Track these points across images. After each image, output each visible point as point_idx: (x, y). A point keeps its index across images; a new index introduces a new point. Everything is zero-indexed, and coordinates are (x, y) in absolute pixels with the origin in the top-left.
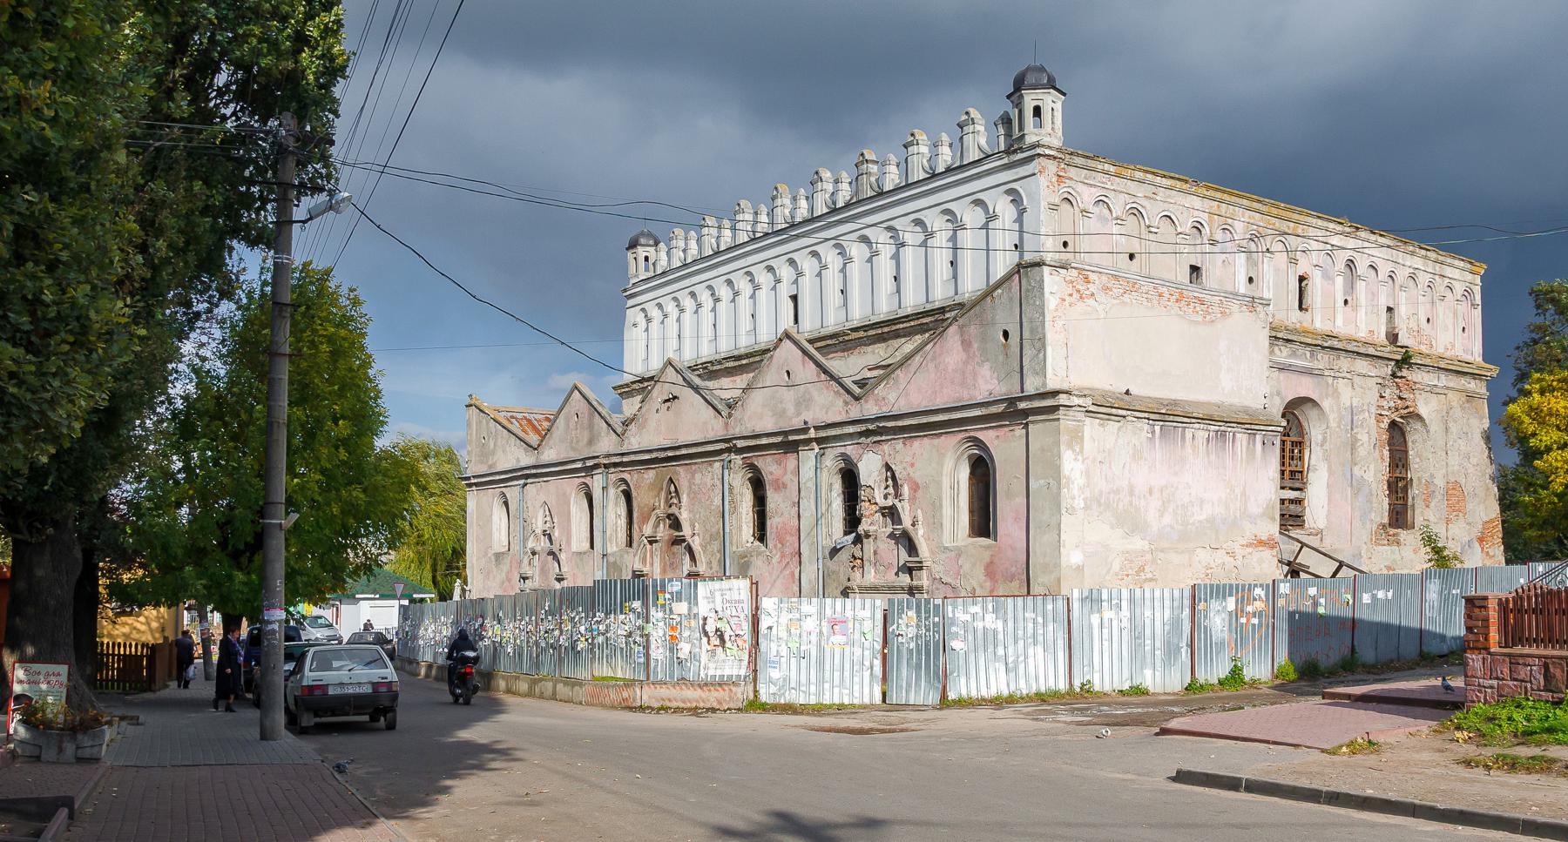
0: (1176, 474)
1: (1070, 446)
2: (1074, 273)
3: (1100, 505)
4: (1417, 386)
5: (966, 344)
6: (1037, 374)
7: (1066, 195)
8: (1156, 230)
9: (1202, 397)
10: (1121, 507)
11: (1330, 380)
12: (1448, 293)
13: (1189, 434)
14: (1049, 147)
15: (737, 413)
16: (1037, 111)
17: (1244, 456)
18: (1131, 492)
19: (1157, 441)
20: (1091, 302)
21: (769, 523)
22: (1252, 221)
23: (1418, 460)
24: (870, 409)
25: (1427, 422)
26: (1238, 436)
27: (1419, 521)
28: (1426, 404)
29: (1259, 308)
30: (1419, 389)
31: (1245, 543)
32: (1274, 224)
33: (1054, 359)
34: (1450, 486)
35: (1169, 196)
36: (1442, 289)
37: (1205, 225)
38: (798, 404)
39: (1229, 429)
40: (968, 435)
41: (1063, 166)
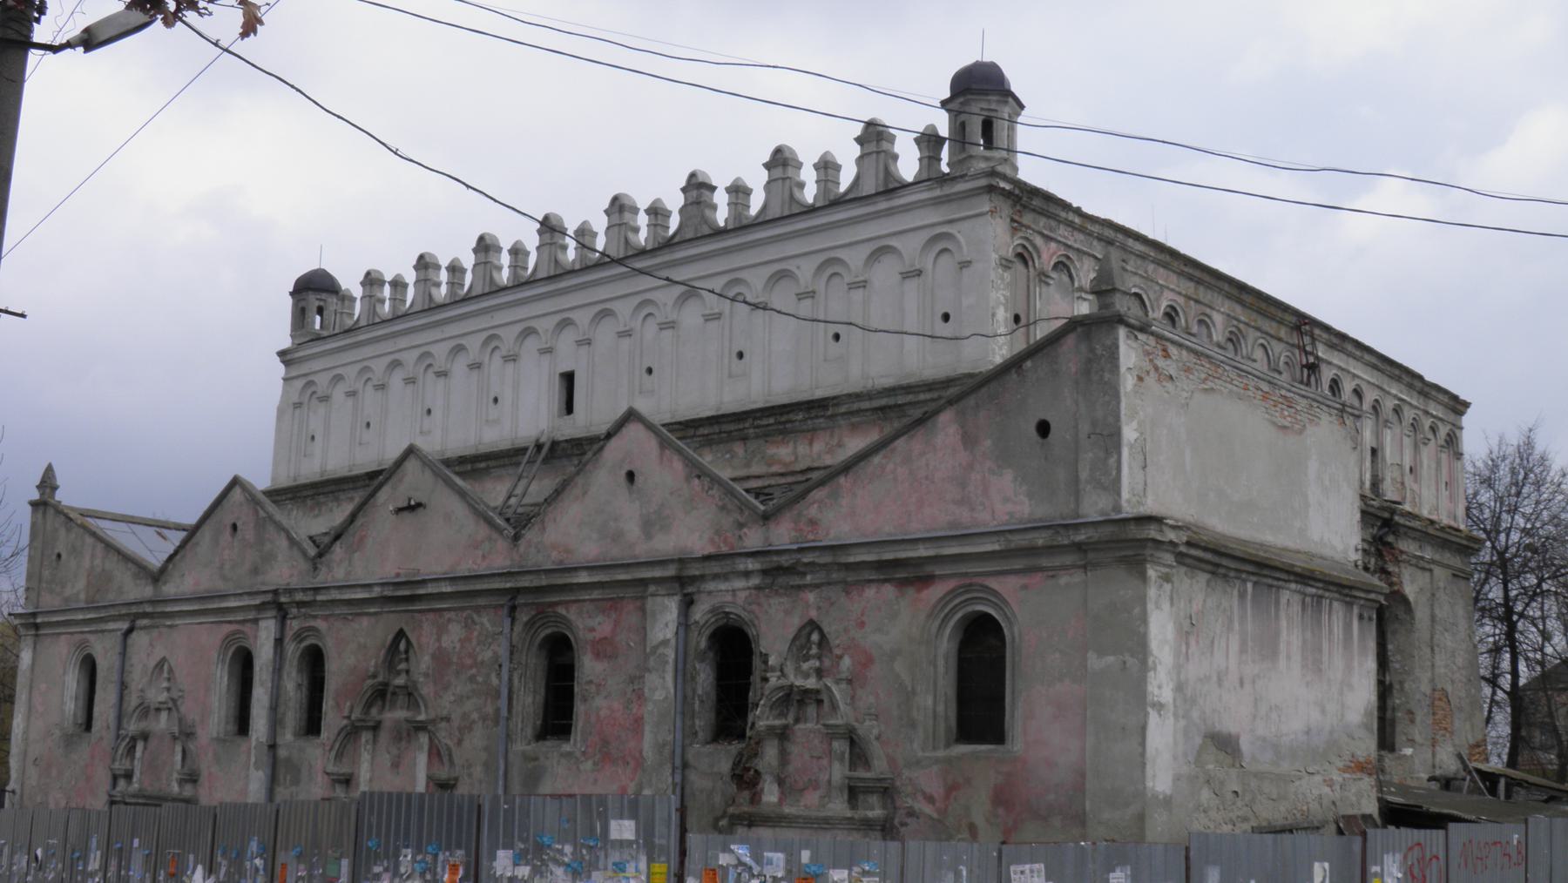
1: (1158, 607)
2: (1152, 341)
5: (969, 440)
6: (1105, 489)
7: (1020, 250)
12: (1430, 436)
13: (1283, 600)
14: (1004, 177)
15: (530, 535)
16: (988, 127)
17: (1341, 636)
20: (1169, 385)
21: (579, 708)
22: (1232, 314)
23: (1398, 657)
24: (782, 534)
25: (1413, 605)
28: (1412, 582)
29: (1349, 421)
30: (1404, 561)
32: (1255, 321)
33: (1130, 468)
34: (1437, 695)
36: (1427, 427)
38: (649, 526)
39: (1327, 594)
40: (968, 581)
41: (1018, 207)
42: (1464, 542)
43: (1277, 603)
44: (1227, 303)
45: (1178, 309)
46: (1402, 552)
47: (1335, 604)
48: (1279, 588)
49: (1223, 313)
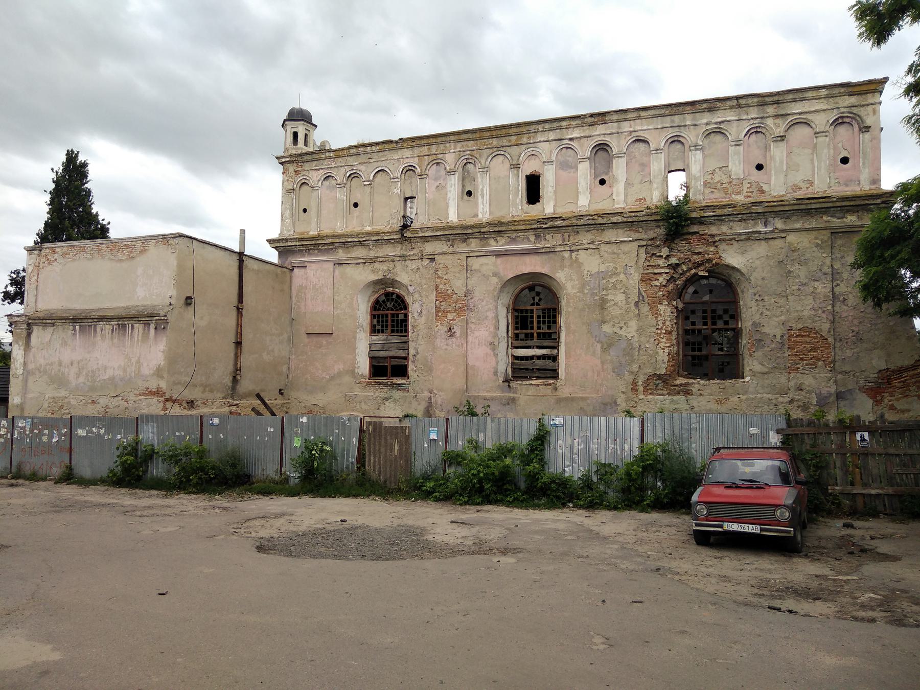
0: (89, 352)
3: (40, 372)
4: (717, 238)
8: (365, 183)
9: (115, 305)
10: (53, 371)
11: (567, 255)
13: (98, 329)
17: (140, 338)
18: (60, 365)
19: (78, 334)
26: (136, 326)
27: (747, 369)
30: (721, 240)
31: (138, 393)
32: (492, 143)
35: (382, 156)
37: (416, 166)
42: (838, 204)
43: (95, 331)
44: (459, 145)
45: (414, 165)
46: (713, 236)
47: (136, 326)
48: (95, 326)
49: (454, 152)
